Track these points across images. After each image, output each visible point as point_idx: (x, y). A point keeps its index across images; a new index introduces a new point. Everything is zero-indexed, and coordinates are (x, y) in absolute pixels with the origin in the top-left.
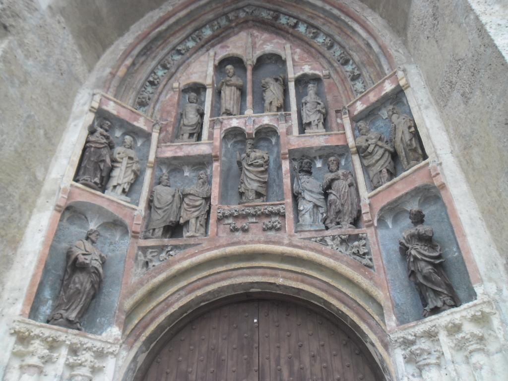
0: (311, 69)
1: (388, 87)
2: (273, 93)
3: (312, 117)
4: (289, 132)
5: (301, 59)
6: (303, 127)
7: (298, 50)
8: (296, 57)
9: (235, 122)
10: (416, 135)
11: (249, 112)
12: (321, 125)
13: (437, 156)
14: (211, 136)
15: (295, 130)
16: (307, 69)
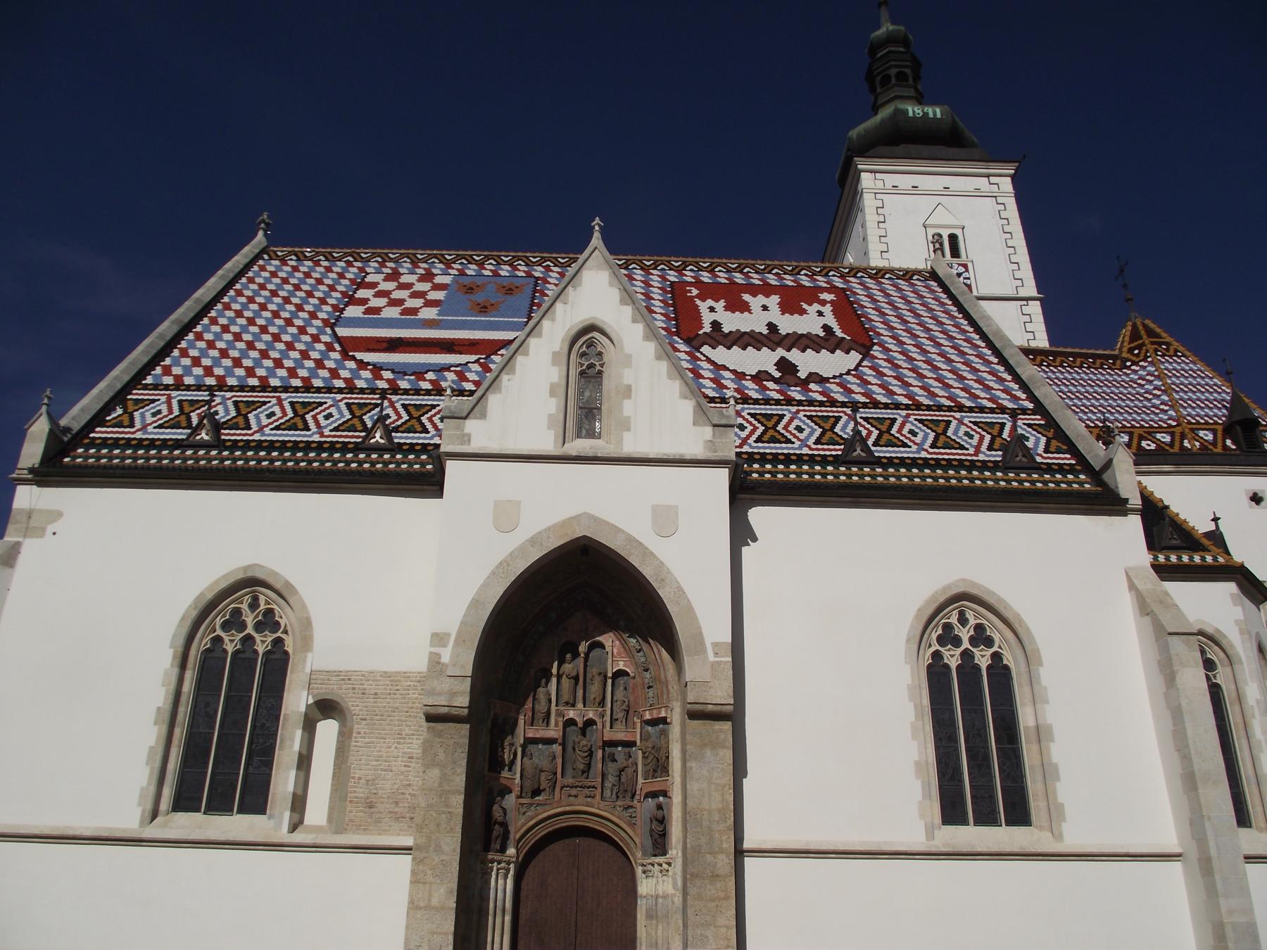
0: (624, 665)
1: (663, 714)
2: (594, 689)
3: (620, 715)
4: (603, 727)
5: (619, 653)
6: (613, 721)
7: (617, 642)
8: (615, 651)
9: (571, 714)
10: (668, 757)
11: (580, 705)
12: (624, 720)
13: (673, 777)
14: (556, 725)
15: (608, 725)
16: (621, 666)
